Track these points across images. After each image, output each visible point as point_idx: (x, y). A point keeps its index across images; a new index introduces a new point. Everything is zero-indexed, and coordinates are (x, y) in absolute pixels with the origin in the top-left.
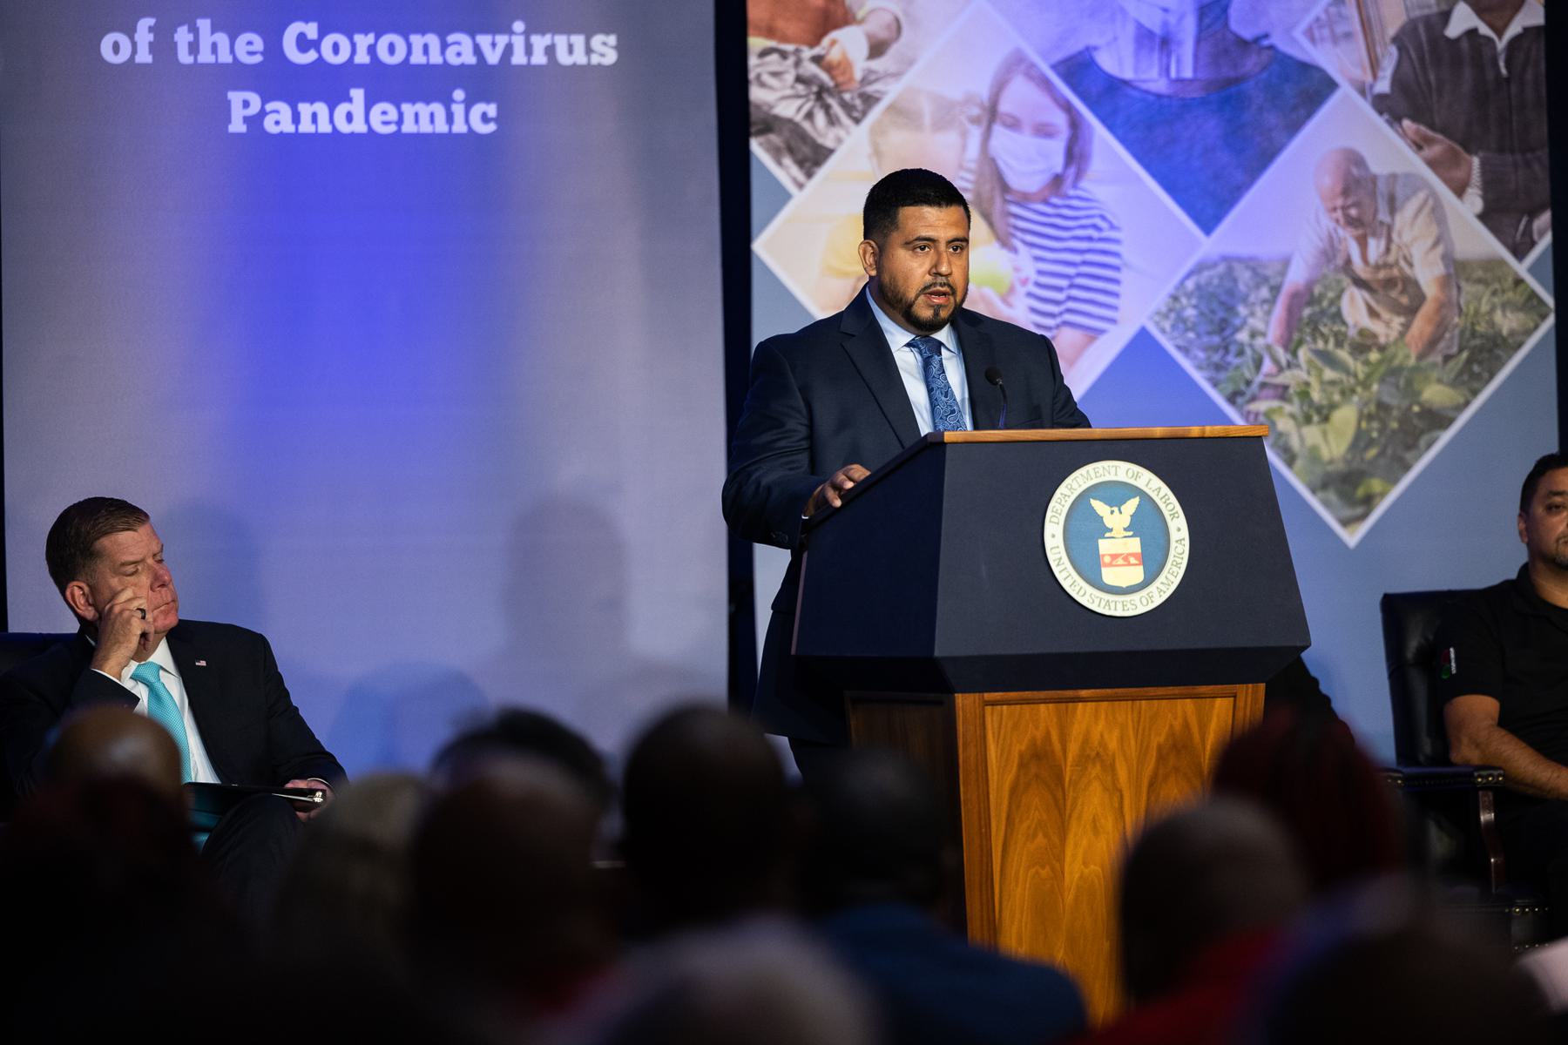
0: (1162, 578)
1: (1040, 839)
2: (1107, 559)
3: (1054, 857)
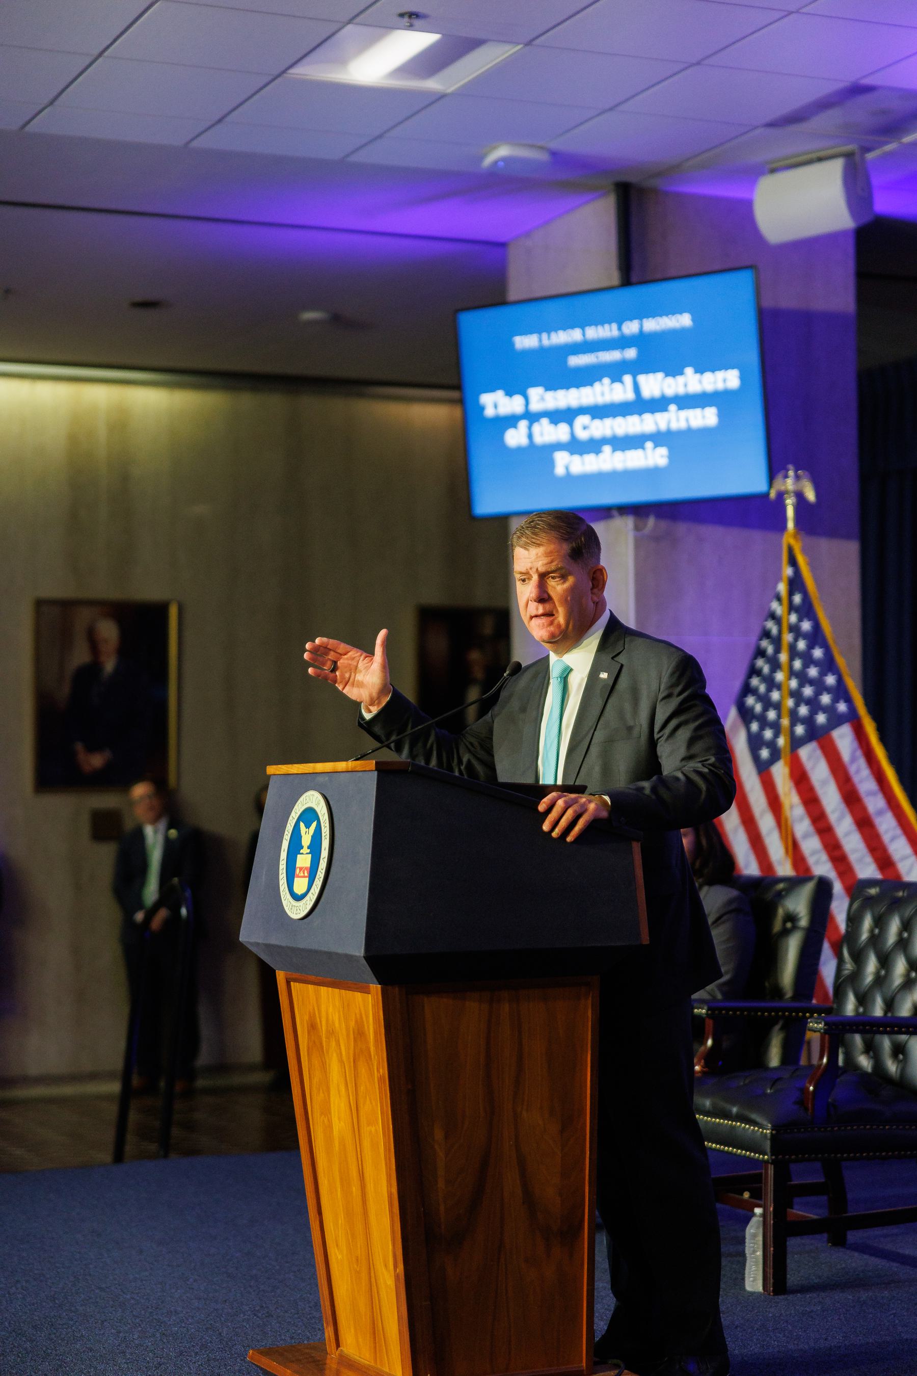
0: (312, 891)
1: (321, 1094)
2: (298, 871)
3: (326, 1111)
